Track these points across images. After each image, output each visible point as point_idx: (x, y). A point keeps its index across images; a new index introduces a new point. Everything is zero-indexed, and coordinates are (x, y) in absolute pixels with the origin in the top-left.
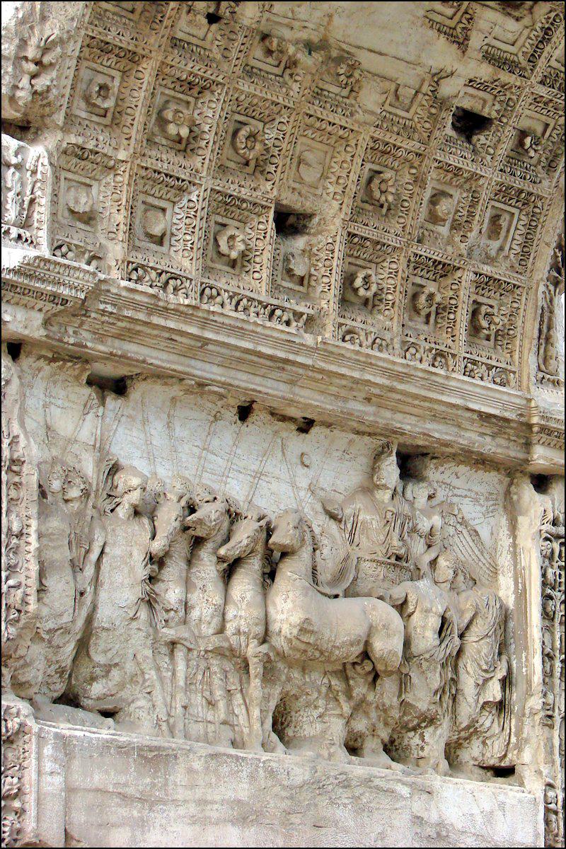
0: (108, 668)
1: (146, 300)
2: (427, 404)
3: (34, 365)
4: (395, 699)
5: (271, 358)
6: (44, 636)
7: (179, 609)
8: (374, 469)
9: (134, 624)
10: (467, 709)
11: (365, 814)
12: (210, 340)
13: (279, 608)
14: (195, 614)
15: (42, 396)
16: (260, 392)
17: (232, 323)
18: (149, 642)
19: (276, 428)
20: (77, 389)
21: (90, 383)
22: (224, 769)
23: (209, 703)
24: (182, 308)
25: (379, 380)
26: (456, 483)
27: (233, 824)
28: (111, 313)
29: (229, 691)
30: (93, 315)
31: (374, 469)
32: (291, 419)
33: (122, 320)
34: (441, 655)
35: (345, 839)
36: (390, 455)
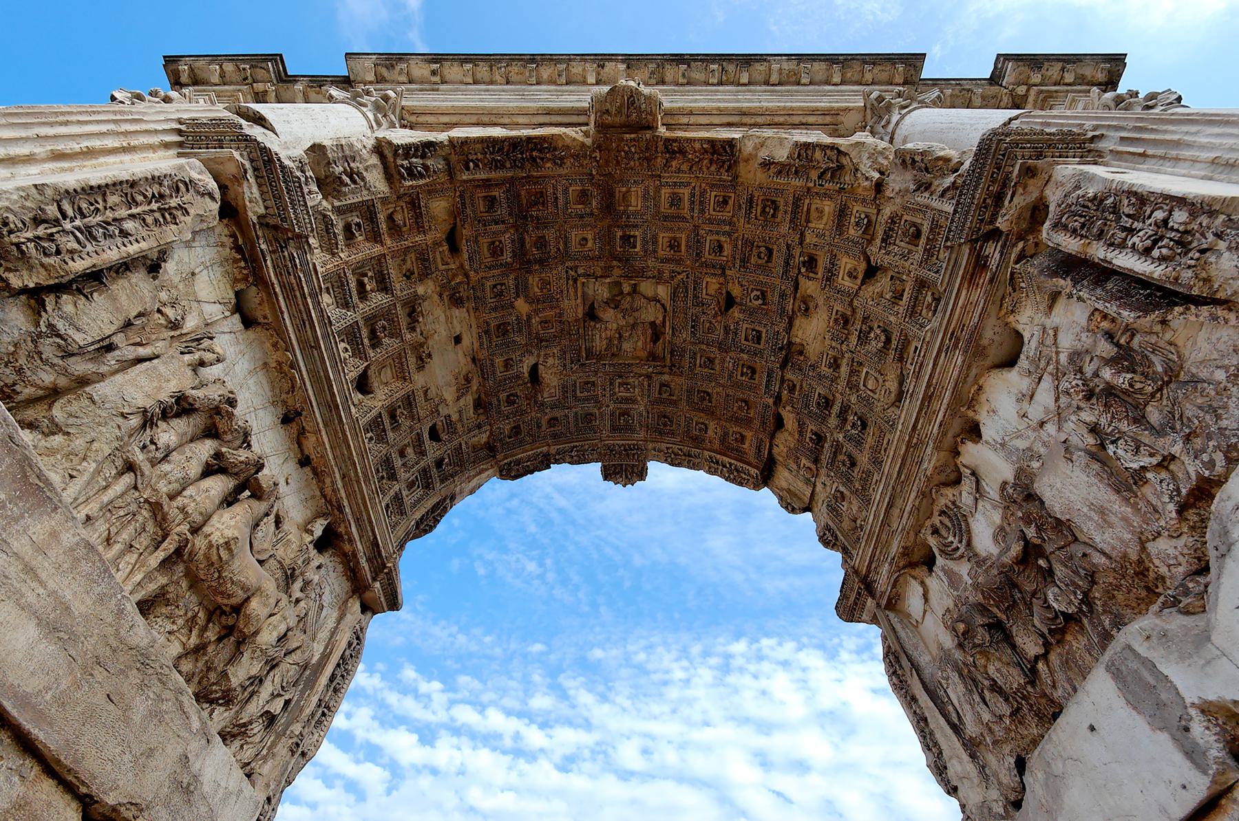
0: (55, 429)
3: (223, 237)
4: (222, 665)
5: (333, 395)
6: (41, 323)
7: (161, 451)
8: (312, 520)
9: (120, 420)
10: (254, 708)
11: (155, 721)
12: (320, 348)
13: (223, 520)
14: (166, 467)
15: (207, 257)
18: (116, 444)
20: (228, 286)
22: (85, 567)
23: (108, 540)
26: (331, 573)
27: (38, 625)
28: (296, 265)
29: (131, 546)
30: (286, 253)
31: (312, 520)
32: (302, 451)
34: (272, 653)
35: (121, 732)
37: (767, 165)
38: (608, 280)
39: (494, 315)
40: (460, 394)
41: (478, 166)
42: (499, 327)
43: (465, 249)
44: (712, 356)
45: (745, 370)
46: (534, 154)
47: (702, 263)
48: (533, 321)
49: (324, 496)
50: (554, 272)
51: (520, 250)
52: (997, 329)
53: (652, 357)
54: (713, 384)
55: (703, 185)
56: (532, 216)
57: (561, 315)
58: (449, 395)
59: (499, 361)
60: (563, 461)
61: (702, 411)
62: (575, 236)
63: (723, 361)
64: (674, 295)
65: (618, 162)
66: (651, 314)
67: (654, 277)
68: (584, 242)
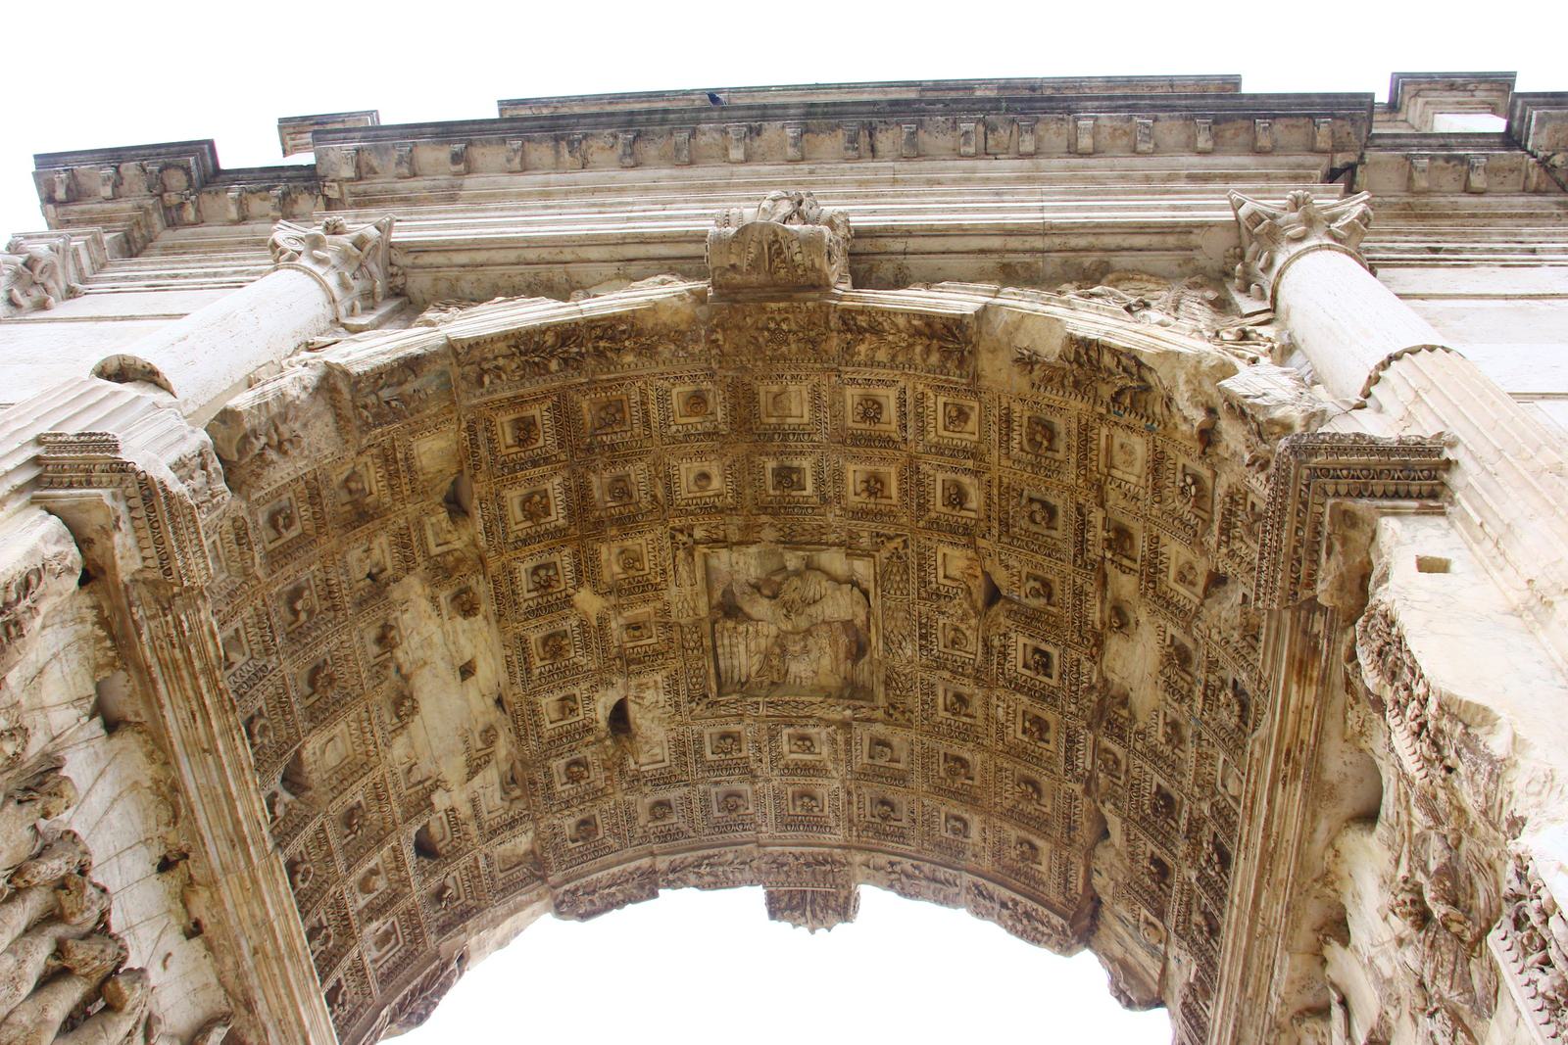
1: (212, 655)
2: (286, 1002)
3: (84, 610)
5: (237, 823)
12: (217, 750)
15: (61, 645)
16: (204, 844)
17: (242, 756)
19: (173, 907)
20: (88, 679)
21: (98, 687)
24: (226, 697)
25: (281, 941)
28: (183, 633)
30: (170, 618)
32: (188, 913)
33: (182, 651)
36: (226, 1025)
37: (1027, 362)
38: (753, 549)
39: (534, 622)
40: (473, 771)
41: (499, 377)
42: (545, 641)
43: (478, 513)
44: (966, 690)
45: (1027, 724)
46: (602, 344)
47: (931, 522)
48: (613, 625)
49: (222, 983)
50: (649, 536)
51: (580, 501)
52: (1347, 758)
53: (853, 690)
54: (971, 745)
55: (920, 388)
56: (602, 445)
57: (666, 613)
58: (453, 769)
59: (548, 703)
60: (685, 883)
61: (955, 794)
62: (686, 471)
63: (987, 704)
64: (882, 577)
65: (759, 348)
66: (840, 606)
67: (840, 545)
68: (704, 483)
